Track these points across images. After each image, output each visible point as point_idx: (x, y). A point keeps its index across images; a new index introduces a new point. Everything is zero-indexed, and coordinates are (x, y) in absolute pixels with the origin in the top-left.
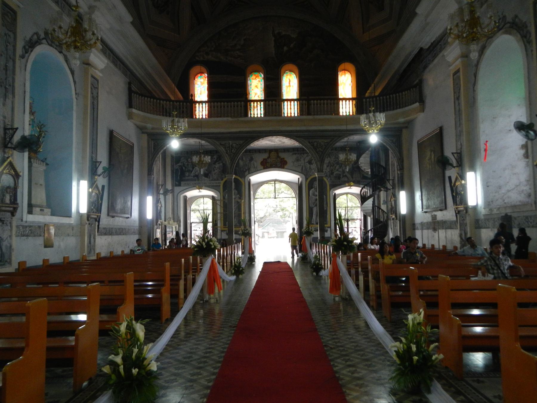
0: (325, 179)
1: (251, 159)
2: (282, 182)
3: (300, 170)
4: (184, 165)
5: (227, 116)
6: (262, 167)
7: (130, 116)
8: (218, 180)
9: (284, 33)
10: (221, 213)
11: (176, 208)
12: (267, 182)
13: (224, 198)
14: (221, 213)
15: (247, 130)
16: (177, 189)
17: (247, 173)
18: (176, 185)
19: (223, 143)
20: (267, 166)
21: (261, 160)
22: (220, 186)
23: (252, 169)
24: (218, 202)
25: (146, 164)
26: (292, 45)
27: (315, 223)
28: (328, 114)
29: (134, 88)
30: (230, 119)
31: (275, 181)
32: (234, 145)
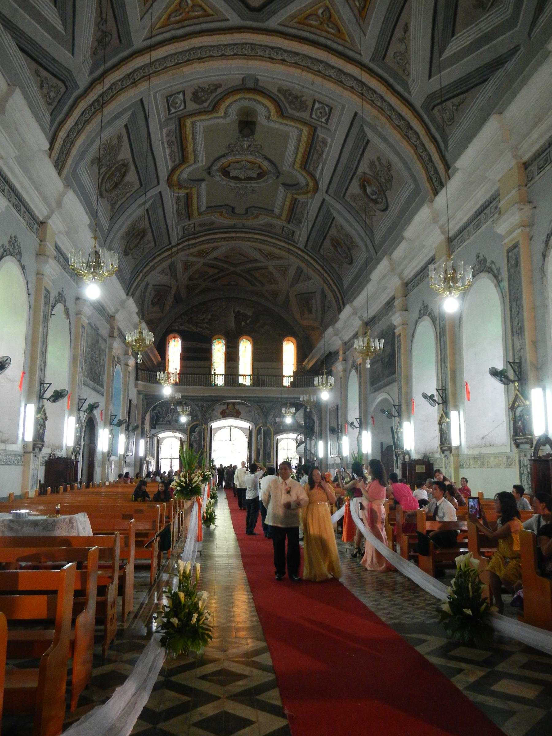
2: (236, 427)
3: (251, 420)
4: (159, 412)
5: (201, 385)
6: (221, 416)
7: (136, 386)
9: (242, 311)
12: (224, 427)
13: (190, 440)
15: (215, 395)
16: (153, 431)
18: (152, 428)
19: (197, 403)
20: (225, 415)
21: (221, 410)
25: (141, 416)
26: (248, 321)
28: (271, 386)
30: (203, 387)
31: (231, 426)
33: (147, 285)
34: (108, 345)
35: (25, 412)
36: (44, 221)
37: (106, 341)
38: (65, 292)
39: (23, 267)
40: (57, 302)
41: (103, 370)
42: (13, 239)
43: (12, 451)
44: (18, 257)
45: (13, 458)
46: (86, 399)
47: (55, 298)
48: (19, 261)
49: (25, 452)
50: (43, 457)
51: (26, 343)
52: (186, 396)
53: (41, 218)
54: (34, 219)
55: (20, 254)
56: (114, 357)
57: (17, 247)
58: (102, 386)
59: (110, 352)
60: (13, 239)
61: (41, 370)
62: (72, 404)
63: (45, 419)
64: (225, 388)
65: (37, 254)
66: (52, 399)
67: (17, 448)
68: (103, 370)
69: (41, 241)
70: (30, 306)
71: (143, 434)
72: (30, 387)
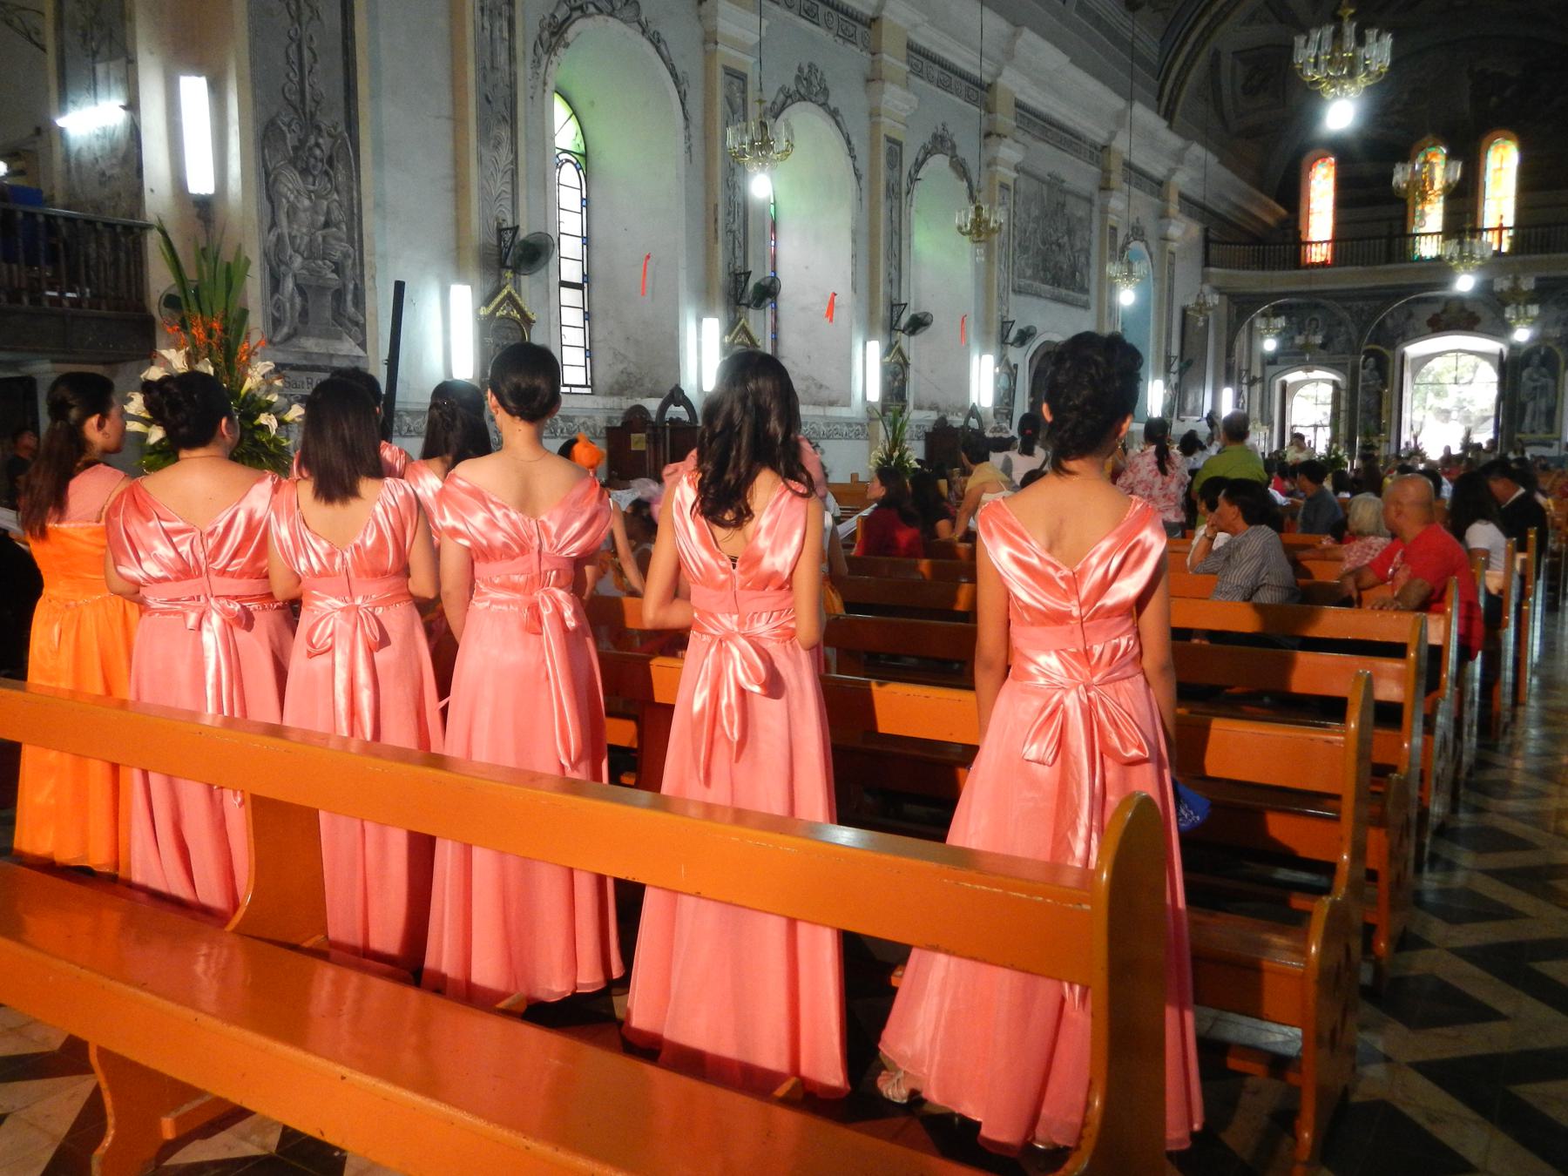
0: (1557, 350)
1: (1410, 316)
5: (1357, 264)
6: (1430, 329)
8: (1344, 353)
10: (1346, 411)
11: (1266, 402)
14: (1346, 411)
17: (1400, 339)
19: (1349, 304)
21: (1428, 317)
22: (1346, 364)
23: (1410, 334)
24: (1343, 394)
25: (1224, 343)
27: (1527, 430)
29: (1211, 236)
30: (1360, 268)
32: (1366, 308)
33: (1216, 55)
34: (1096, 210)
35: (864, 355)
36: (875, 15)
37: (1090, 201)
38: (951, 131)
39: (834, 114)
40: (928, 153)
41: (1083, 259)
42: (806, 70)
43: (840, 417)
44: (821, 99)
45: (845, 428)
46: (1013, 322)
47: (924, 147)
48: (824, 105)
49: (871, 419)
50: (917, 426)
51: (854, 241)
52: (1326, 291)
53: (869, 13)
54: (856, 19)
55: (825, 92)
56: (1114, 229)
57: (815, 82)
58: (1084, 290)
59: (1104, 220)
60: (806, 70)
61: (891, 281)
62: (987, 333)
63: (905, 364)
64: (1512, 258)
65: (869, 80)
66: (911, 329)
67: (855, 411)
68: (1083, 259)
69: (873, 54)
70: (858, 176)
71: (1229, 375)
72: (872, 312)
